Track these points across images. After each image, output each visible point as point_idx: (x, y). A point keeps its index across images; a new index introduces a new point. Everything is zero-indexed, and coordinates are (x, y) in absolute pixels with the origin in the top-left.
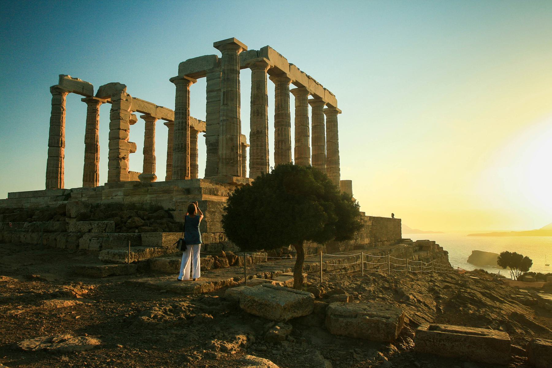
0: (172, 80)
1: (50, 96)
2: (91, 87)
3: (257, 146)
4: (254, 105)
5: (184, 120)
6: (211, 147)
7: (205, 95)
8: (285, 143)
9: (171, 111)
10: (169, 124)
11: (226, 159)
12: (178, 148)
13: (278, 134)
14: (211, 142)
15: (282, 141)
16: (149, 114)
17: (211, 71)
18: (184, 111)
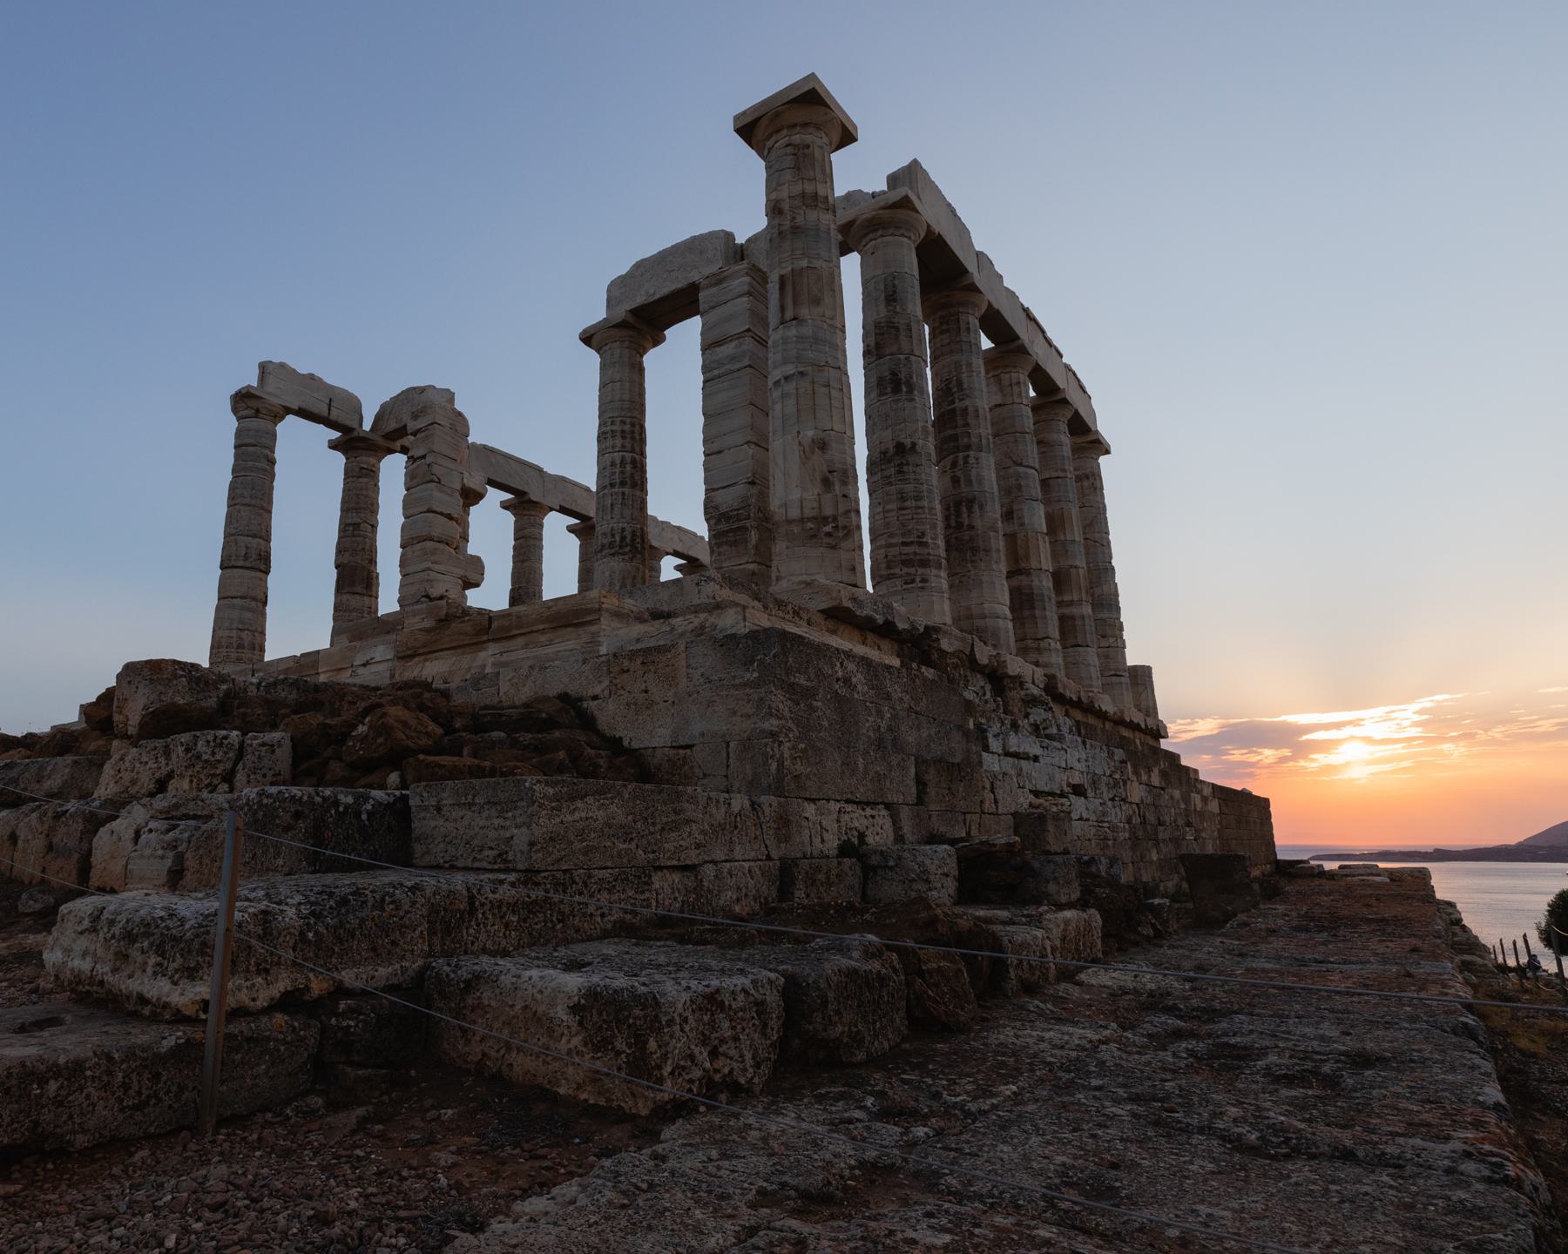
0: (588, 338)
1: (232, 423)
2: (356, 407)
3: (903, 499)
4: (879, 357)
5: (628, 456)
6: (723, 527)
7: (697, 360)
8: (981, 507)
9: (588, 490)
10: (584, 529)
11: (802, 520)
12: (611, 545)
13: (955, 481)
14: (723, 509)
15: (971, 502)
16: (524, 493)
17: (718, 279)
18: (627, 428)
